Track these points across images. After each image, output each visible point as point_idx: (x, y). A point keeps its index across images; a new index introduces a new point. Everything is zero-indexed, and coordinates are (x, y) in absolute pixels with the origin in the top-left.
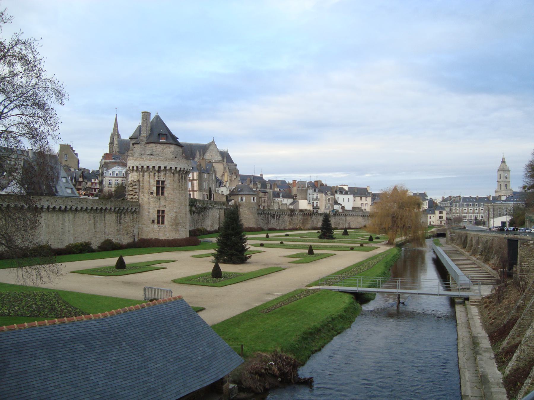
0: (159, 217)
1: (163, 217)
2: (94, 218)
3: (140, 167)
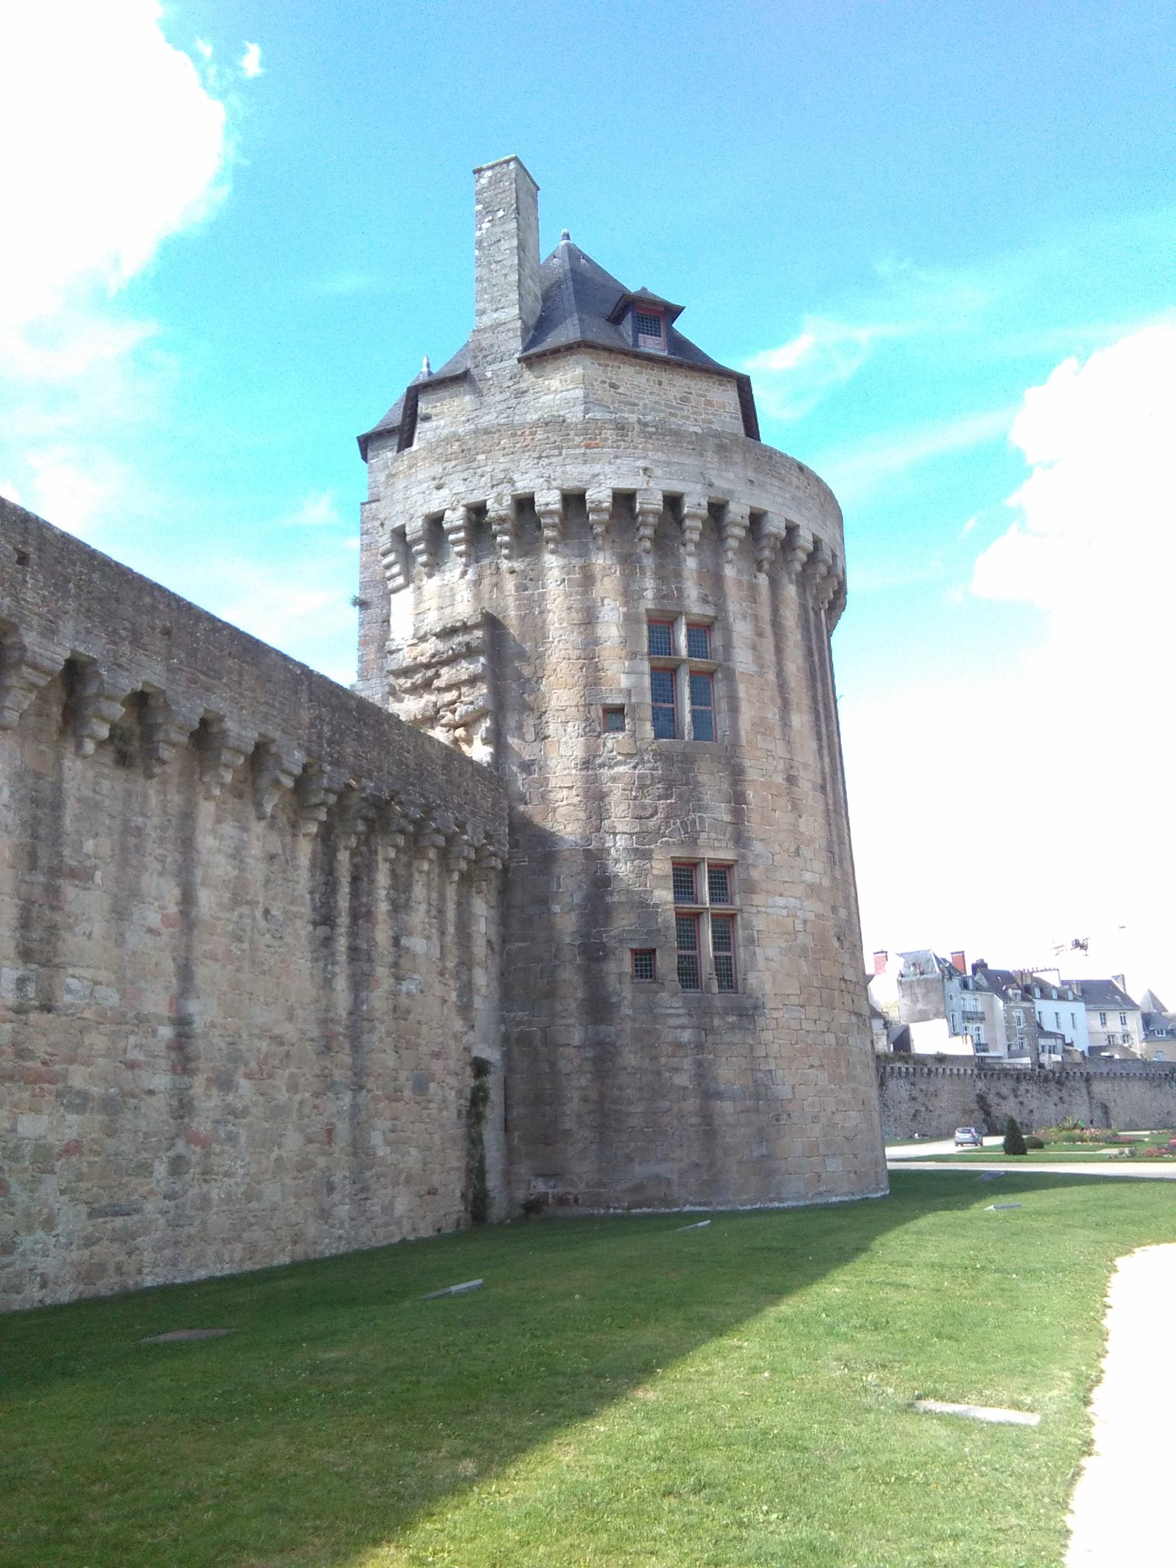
0: (688, 922)
1: (725, 926)
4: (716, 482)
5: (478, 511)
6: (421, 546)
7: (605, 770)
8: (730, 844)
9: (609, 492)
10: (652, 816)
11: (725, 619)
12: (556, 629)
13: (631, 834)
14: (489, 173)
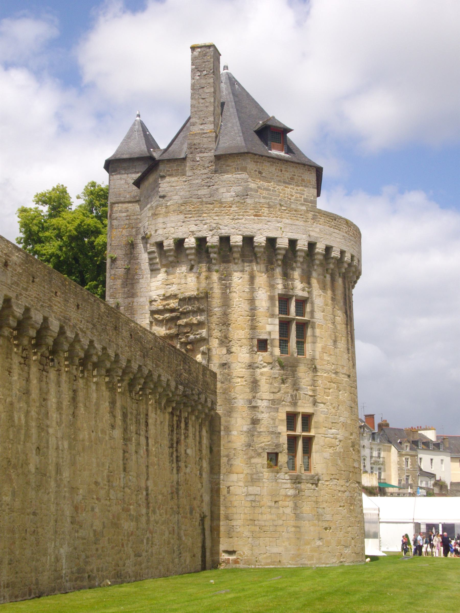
0: (292, 440)
2: (125, 415)
3: (213, 240)
4: (312, 234)
5: (201, 241)
6: (172, 253)
7: (258, 370)
8: (311, 405)
9: (265, 239)
10: (279, 392)
11: (312, 298)
12: (237, 301)
13: (269, 400)
14: (199, 50)
